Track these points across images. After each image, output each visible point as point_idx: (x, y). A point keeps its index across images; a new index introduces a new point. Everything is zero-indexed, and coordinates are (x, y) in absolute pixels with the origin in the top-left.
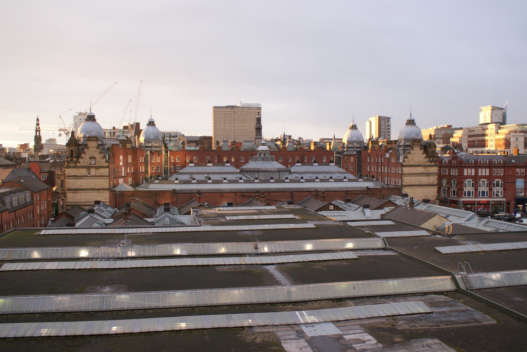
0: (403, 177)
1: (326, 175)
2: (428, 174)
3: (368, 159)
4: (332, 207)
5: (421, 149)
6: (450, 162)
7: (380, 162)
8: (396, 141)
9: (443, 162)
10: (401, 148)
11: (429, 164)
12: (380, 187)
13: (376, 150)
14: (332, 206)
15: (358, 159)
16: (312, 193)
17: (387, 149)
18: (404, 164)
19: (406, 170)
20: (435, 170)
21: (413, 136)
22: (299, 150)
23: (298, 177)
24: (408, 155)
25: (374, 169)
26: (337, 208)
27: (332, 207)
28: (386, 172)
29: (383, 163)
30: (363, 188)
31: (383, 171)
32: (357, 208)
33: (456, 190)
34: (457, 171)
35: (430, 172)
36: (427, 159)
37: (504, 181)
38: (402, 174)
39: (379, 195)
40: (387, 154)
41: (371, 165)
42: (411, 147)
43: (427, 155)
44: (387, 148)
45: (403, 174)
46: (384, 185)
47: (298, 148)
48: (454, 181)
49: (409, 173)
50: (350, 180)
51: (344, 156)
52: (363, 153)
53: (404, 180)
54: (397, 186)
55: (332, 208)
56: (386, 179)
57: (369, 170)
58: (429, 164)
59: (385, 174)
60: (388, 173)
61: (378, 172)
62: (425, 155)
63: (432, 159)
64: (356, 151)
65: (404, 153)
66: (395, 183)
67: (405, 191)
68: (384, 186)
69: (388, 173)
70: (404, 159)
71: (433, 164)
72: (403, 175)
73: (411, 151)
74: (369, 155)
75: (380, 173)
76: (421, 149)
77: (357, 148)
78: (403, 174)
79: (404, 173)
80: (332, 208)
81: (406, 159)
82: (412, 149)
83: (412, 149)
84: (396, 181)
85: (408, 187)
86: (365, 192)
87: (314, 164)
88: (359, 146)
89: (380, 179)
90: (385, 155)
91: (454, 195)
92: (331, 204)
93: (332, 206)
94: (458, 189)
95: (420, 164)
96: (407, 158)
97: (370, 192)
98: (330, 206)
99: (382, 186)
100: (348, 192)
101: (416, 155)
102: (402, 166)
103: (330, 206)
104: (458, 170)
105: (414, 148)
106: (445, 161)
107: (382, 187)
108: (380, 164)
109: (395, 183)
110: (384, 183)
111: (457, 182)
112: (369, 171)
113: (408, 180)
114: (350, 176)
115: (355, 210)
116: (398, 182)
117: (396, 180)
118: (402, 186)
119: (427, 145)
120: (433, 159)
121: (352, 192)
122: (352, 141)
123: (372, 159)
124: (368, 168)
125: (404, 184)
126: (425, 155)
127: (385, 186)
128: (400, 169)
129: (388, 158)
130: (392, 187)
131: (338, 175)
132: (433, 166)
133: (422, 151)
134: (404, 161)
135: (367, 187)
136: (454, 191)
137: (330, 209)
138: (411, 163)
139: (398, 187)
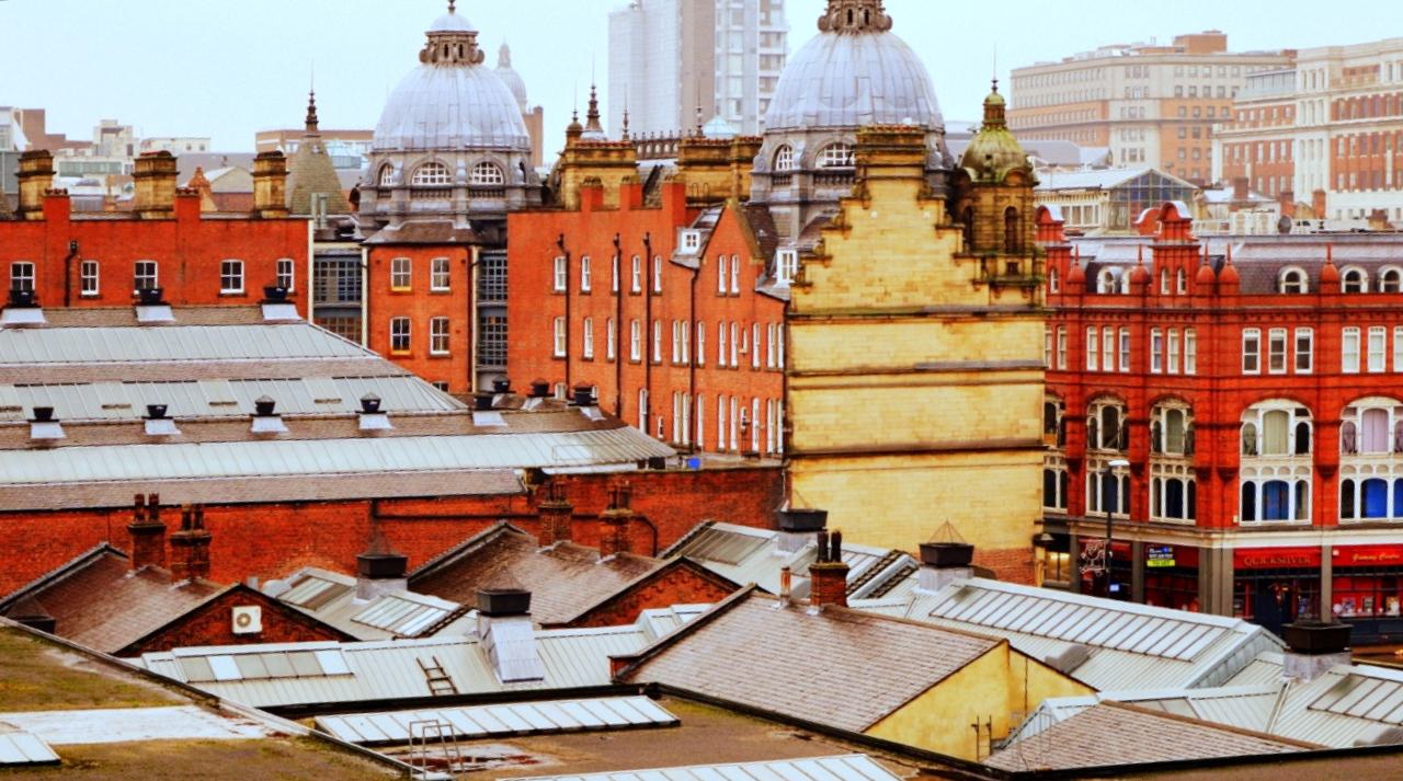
0: (792, 394)
1: (227, 390)
2: (975, 374)
3: (559, 271)
4: (249, 618)
5: (924, 197)
6: (1143, 283)
7: (636, 288)
8: (754, 144)
9: (1101, 289)
10: (784, 193)
11: (983, 298)
12: (634, 467)
13: (611, 209)
14: (254, 612)
15: (482, 272)
16: (115, 519)
17: (690, 200)
18: (802, 301)
19: (815, 346)
20: (1026, 339)
21: (868, 112)
22: (40, 215)
23: (19, 409)
24: (834, 243)
25: (601, 344)
26: (288, 623)
27: (249, 618)
29: (656, 301)
30: (504, 472)
31: (657, 358)
32: (439, 615)
33: (1185, 478)
34: (1191, 349)
35: (993, 358)
36: (971, 268)
37: (1316, 415)
38: (789, 373)
39: (608, 520)
40: (684, 234)
41: (575, 316)
42: (856, 179)
43: (970, 239)
44: (689, 193)
45: (797, 375)
47: (32, 201)
48: (1174, 415)
49: (840, 365)
50: (410, 424)
51: (378, 253)
52: (522, 232)
53: (798, 417)
54: (757, 455)
55: (256, 626)
57: (560, 353)
58: (983, 298)
59: (675, 371)
61: (625, 366)
62: (953, 240)
63: (1002, 265)
64: (470, 214)
65: (806, 231)
66: (745, 435)
67: (810, 488)
68: (657, 462)
70: (802, 269)
71: (1012, 298)
72: (792, 382)
73: (854, 211)
74: (561, 244)
75: (642, 370)
76: (924, 197)
77: (474, 191)
78: (797, 375)
79: (801, 364)
80: (256, 626)
81: (815, 271)
82: (862, 197)
83: (862, 197)
84: (748, 425)
85: (832, 464)
86: (520, 506)
87: (140, 310)
88: (490, 178)
89: (643, 412)
90: (675, 244)
91: (1175, 510)
92: (246, 595)
93: (254, 612)
94: (1203, 473)
95: (922, 299)
96: (824, 259)
97: (546, 504)
98: (237, 611)
99: (641, 463)
100: (384, 510)
101: (891, 236)
102: (791, 316)
103: (237, 611)
104: (1198, 339)
105: (875, 188)
106: (1109, 276)
107: (647, 469)
108: (636, 308)
109: (745, 435)
110: (667, 438)
111: (1196, 426)
112: (567, 359)
113: (831, 418)
114: (408, 393)
115: (426, 634)
116: (764, 432)
117: (749, 412)
118: (791, 453)
119: (971, 172)
120: (1012, 268)
121: (422, 509)
122: (443, 143)
123: (584, 273)
124: (559, 332)
125: (801, 440)
126: (953, 240)
127: (672, 463)
128: (775, 334)
130: (722, 462)
131: (327, 387)
132: (1019, 313)
133: (934, 212)
134: (801, 283)
135: (536, 474)
136: (1174, 486)
137: (237, 629)
138: (853, 298)
139: (765, 463)
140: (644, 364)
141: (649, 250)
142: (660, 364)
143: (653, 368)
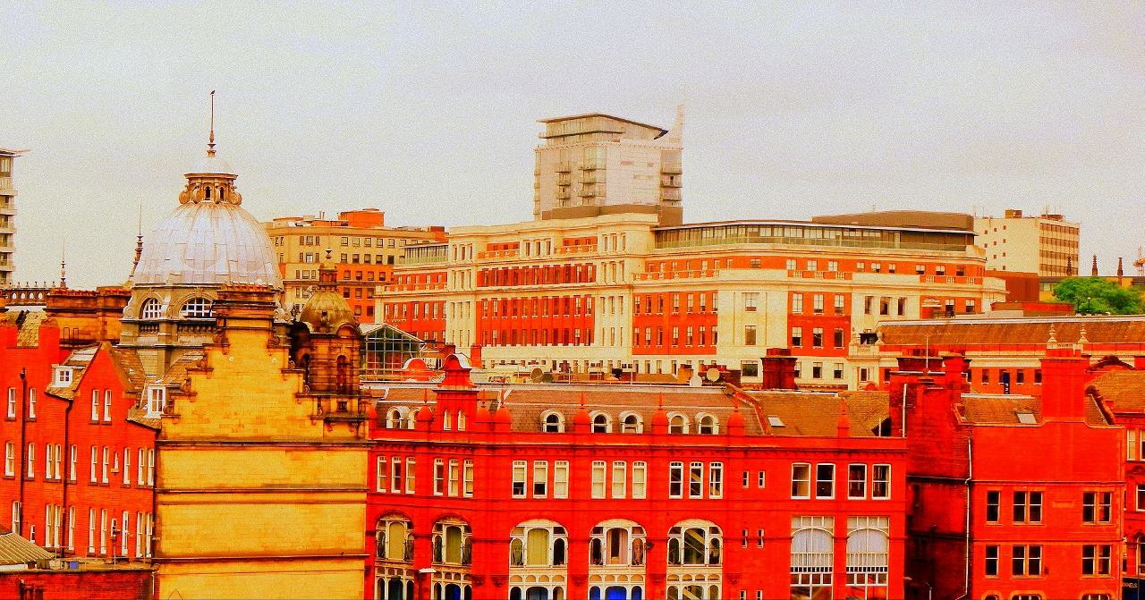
12: (24, 567)
28: (53, 481)
31: (31, 475)
46: (41, 553)
56: (53, 518)
59: (49, 487)
60: (65, 482)
68: (44, 564)
69: (65, 482)
89: (15, 519)
90: (49, 378)
99: (31, 564)
110: (40, 540)
129: (68, 395)
140: (18, 479)
141: (25, 384)
142: (32, 480)
143: (26, 483)
